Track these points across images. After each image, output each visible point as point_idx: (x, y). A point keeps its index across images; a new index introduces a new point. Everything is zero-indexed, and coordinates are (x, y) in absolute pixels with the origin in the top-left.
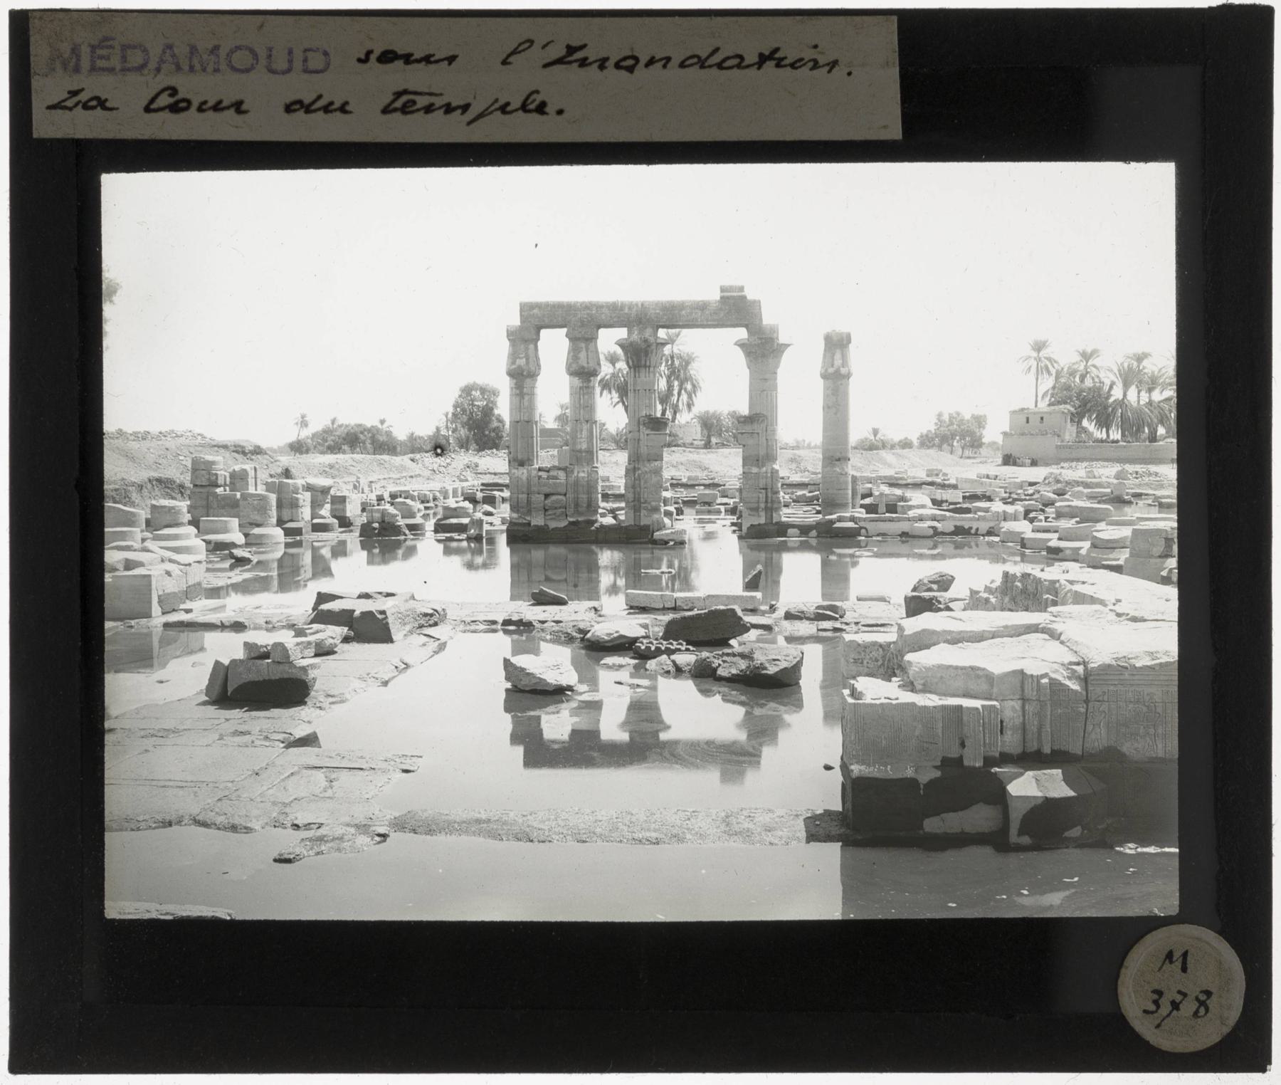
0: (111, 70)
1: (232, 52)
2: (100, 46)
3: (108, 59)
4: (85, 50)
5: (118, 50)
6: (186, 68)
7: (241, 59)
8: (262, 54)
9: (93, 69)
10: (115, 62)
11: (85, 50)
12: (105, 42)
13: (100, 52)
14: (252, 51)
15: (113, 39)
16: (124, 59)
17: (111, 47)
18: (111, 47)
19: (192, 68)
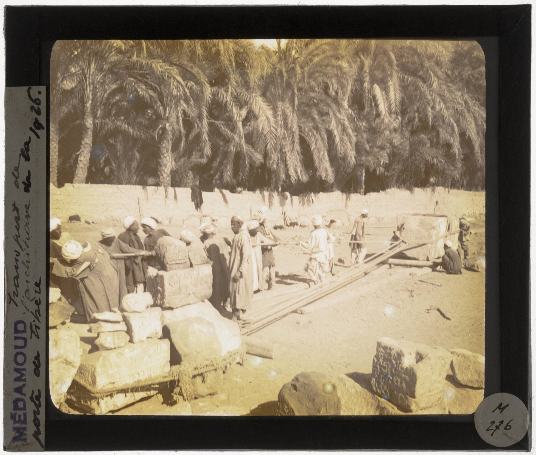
0: (25, 415)
1: (17, 363)
2: (15, 420)
3: (20, 416)
4: (17, 425)
5: (15, 412)
6: (24, 383)
7: (20, 359)
8: (18, 350)
9: (25, 422)
10: (21, 413)
11: (17, 425)
12: (13, 417)
13: (17, 418)
14: (17, 354)
15: (11, 413)
16: (20, 409)
17: (15, 414)
18: (15, 414)
19: (25, 380)
